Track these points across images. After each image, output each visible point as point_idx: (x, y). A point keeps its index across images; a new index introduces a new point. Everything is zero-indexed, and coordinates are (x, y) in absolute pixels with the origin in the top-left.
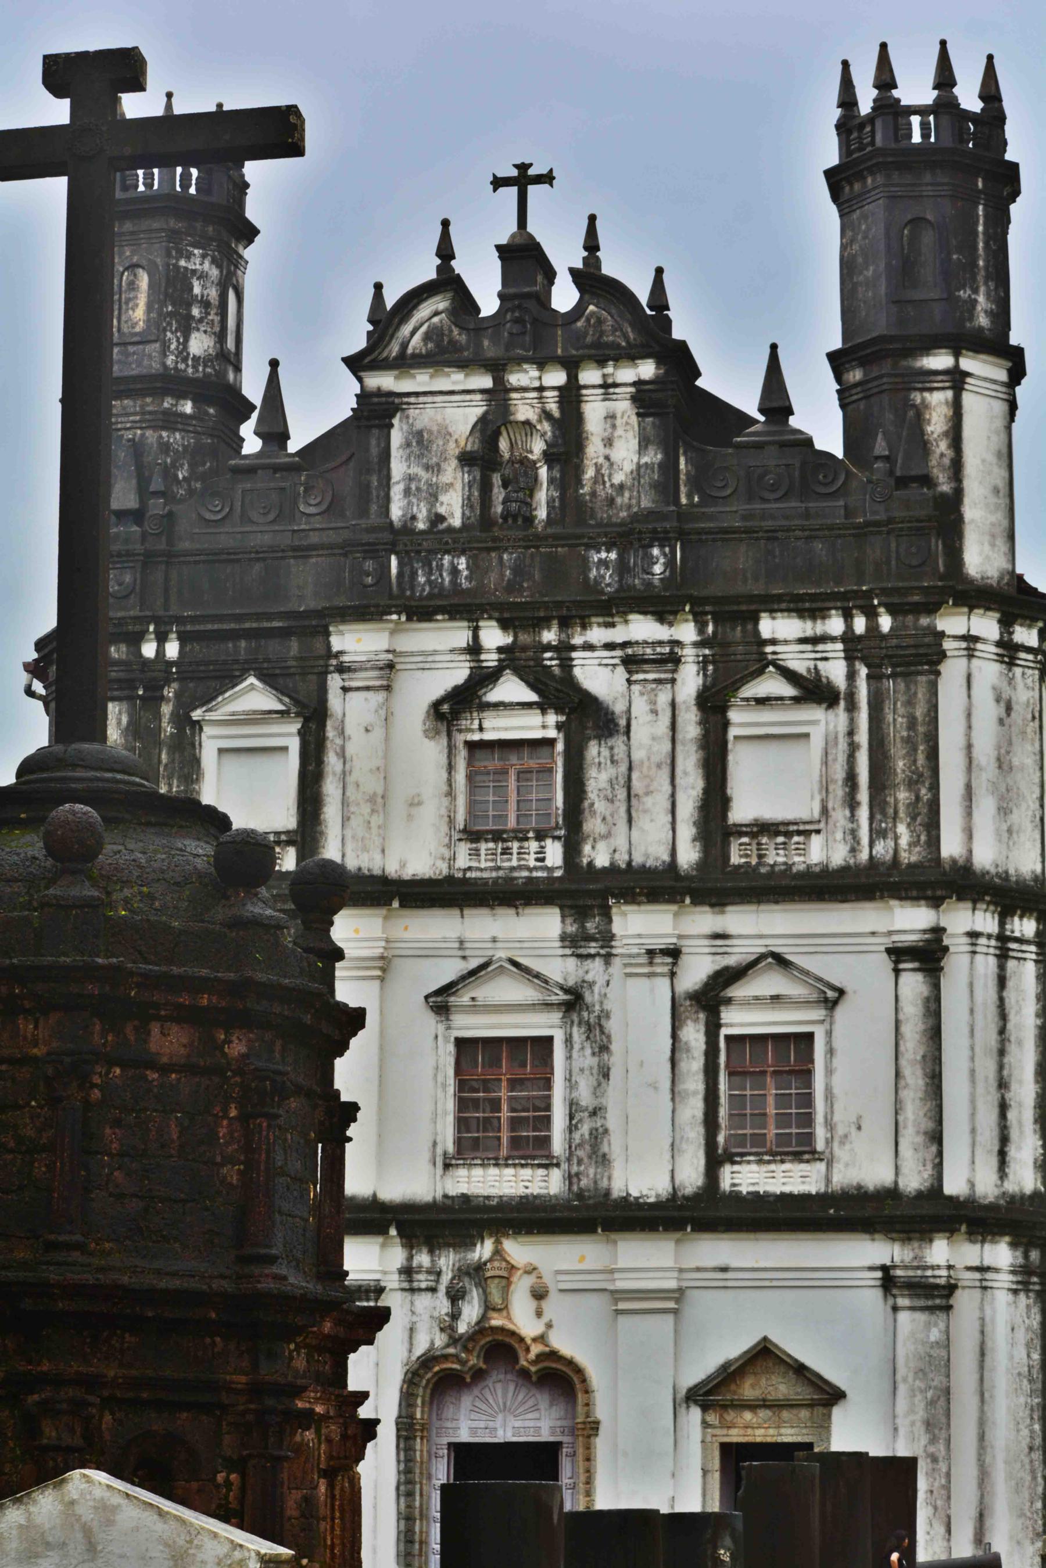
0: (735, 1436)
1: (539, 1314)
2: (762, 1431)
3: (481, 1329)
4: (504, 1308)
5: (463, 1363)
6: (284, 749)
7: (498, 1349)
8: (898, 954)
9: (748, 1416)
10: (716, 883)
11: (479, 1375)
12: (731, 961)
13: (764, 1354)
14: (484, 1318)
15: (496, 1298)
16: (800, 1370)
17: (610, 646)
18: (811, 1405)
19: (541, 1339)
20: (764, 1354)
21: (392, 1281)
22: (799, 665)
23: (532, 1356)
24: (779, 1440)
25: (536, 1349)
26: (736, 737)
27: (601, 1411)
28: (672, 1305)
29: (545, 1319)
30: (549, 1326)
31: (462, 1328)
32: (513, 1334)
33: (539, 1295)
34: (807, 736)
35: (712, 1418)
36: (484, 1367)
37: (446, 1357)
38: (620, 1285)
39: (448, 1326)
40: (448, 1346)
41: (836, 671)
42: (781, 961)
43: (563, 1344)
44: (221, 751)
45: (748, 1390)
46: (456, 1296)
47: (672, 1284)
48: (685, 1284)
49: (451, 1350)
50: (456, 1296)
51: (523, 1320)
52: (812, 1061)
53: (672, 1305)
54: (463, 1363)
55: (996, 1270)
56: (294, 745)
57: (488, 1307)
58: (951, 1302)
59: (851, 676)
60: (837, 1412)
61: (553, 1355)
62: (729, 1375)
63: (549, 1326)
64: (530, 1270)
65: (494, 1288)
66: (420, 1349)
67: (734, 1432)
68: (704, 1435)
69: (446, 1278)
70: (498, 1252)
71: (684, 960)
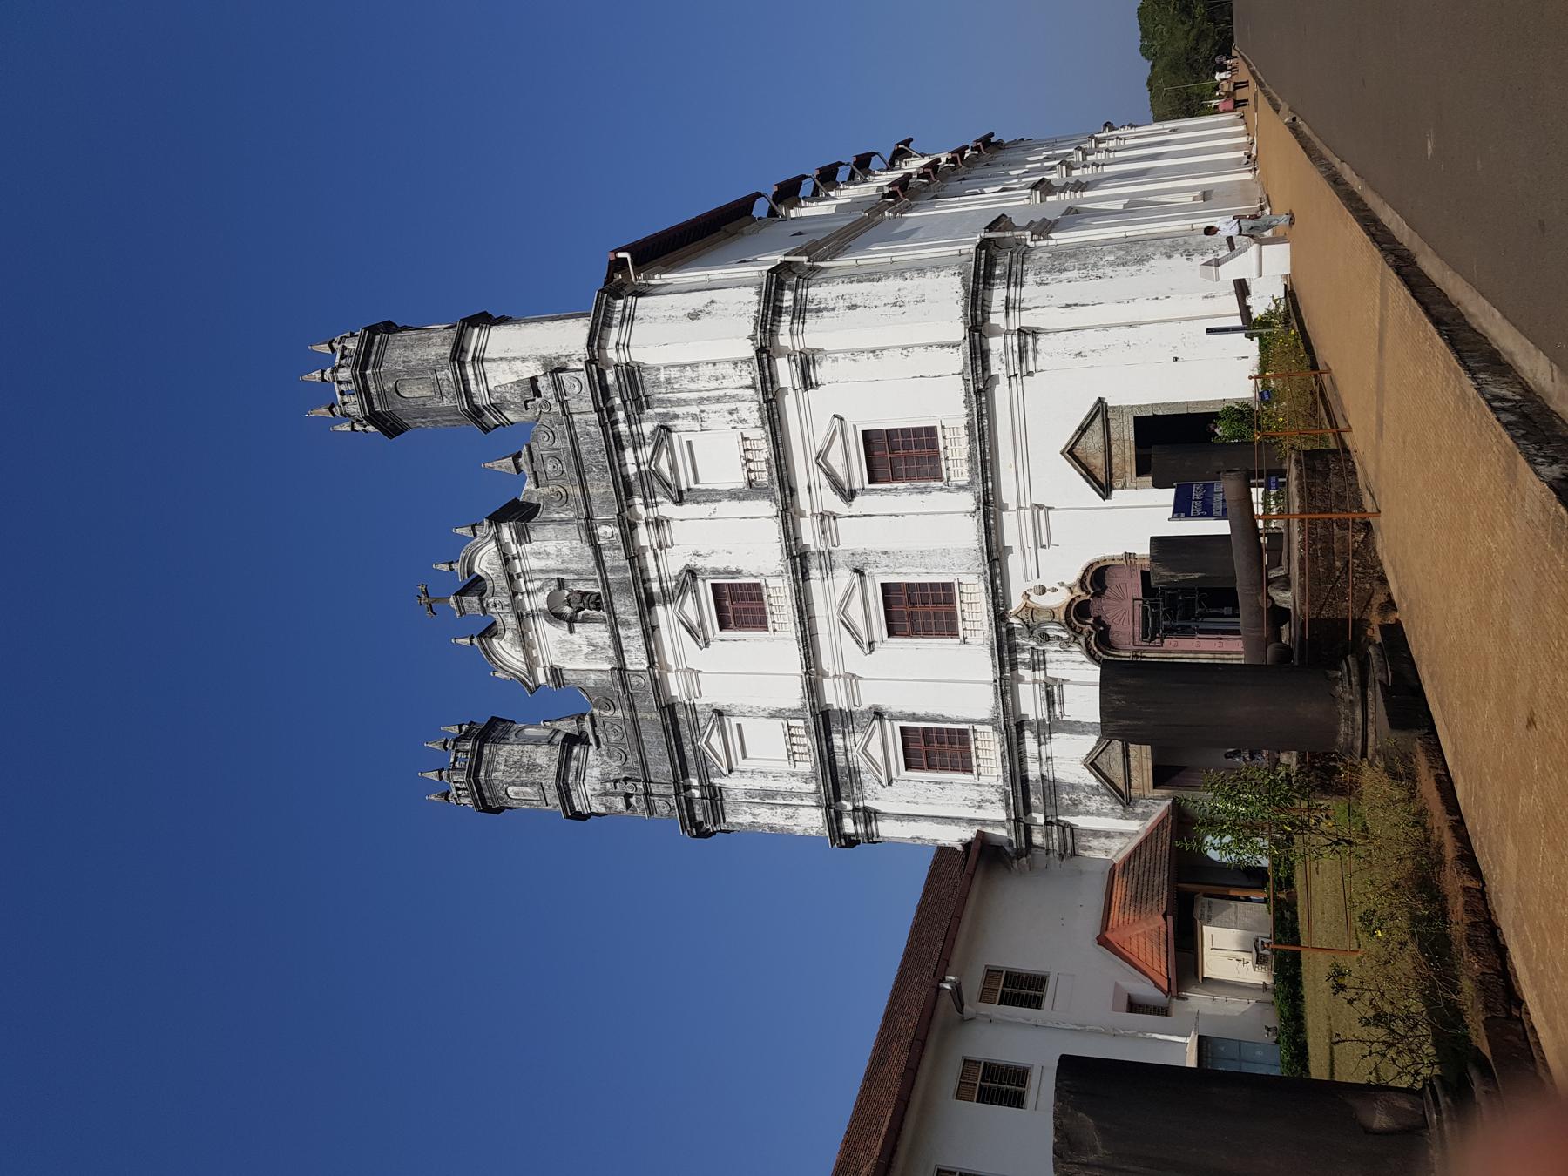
0: (1131, 468)
1: (1055, 590)
5: (1090, 633)
6: (739, 726)
7: (1078, 612)
8: (808, 383)
9: (1115, 460)
10: (783, 487)
11: (1098, 620)
12: (824, 481)
13: (1071, 453)
16: (1083, 430)
17: (656, 556)
20: (1071, 453)
21: (1040, 675)
22: (649, 450)
26: (696, 482)
30: (1062, 584)
32: (1069, 605)
33: (1043, 590)
34: (689, 443)
35: (1117, 483)
36: (1091, 621)
37: (1087, 643)
38: (1031, 544)
39: (1066, 645)
41: (647, 428)
42: (822, 456)
43: (1074, 576)
44: (744, 757)
45: (1097, 462)
46: (1046, 638)
47: (1029, 513)
49: (1082, 640)
50: (1046, 638)
51: (1059, 600)
54: (1090, 633)
55: (1007, 298)
56: (734, 721)
59: (650, 419)
61: (1082, 582)
62: (1089, 474)
63: (1062, 584)
65: (1040, 618)
66: (1084, 658)
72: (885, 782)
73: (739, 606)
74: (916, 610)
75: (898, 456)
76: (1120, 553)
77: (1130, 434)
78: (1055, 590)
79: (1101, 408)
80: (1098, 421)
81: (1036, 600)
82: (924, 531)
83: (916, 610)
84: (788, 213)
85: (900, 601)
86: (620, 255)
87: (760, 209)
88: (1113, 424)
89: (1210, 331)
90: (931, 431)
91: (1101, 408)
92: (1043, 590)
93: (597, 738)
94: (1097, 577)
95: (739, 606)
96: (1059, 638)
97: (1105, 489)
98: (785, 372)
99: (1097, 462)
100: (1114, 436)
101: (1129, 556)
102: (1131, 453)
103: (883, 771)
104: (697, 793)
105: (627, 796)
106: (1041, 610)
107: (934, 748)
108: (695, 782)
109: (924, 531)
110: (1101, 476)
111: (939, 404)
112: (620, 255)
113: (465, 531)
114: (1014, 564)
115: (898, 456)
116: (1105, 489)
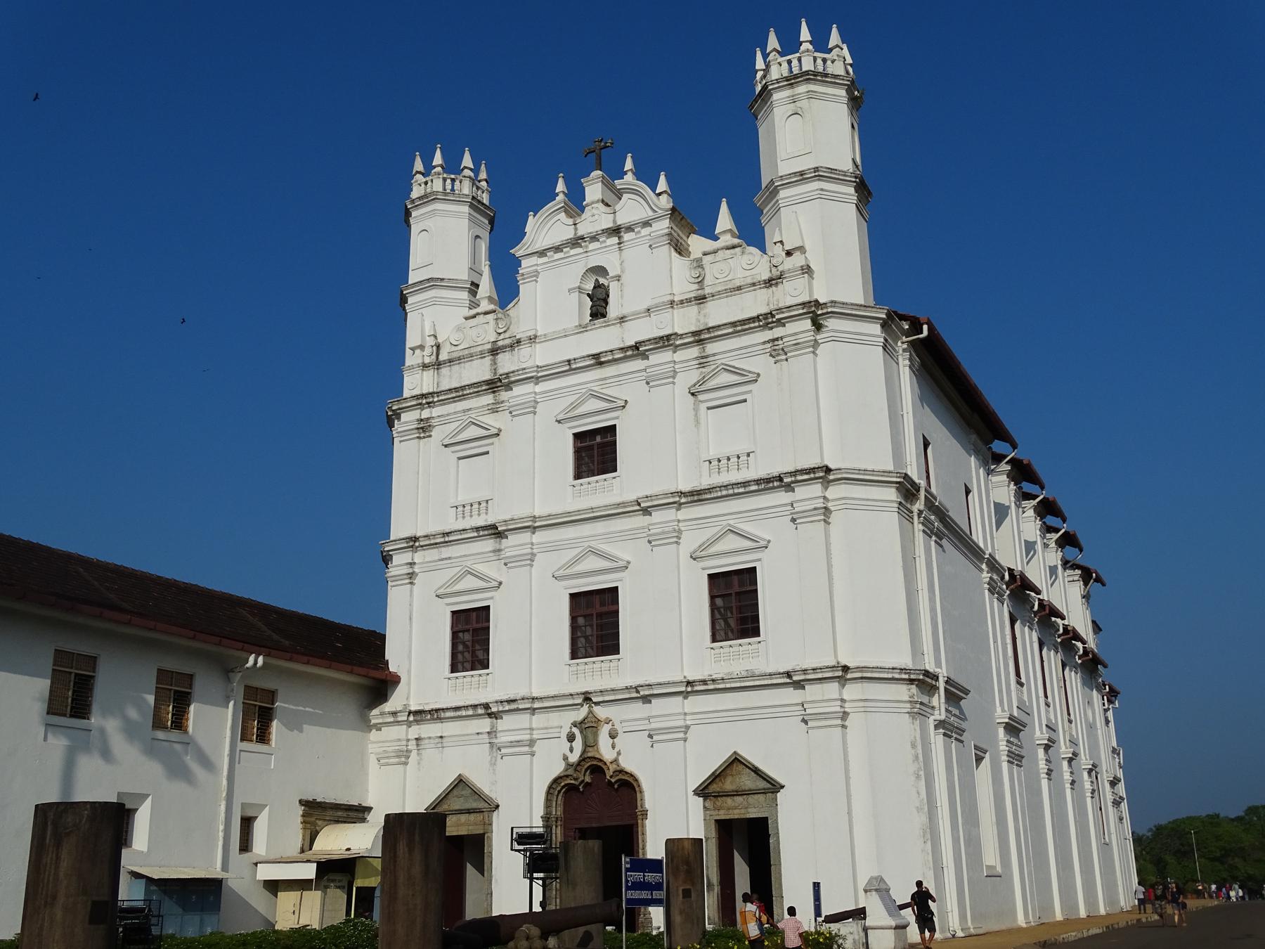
0: (723, 815)
1: (613, 747)
2: (736, 811)
3: (583, 759)
4: (595, 745)
5: (576, 779)
7: (596, 767)
9: (729, 800)
13: (736, 761)
14: (584, 752)
15: (591, 742)
16: (756, 771)
18: (764, 792)
19: (615, 761)
20: (736, 761)
23: (612, 770)
24: (748, 816)
25: (613, 768)
27: (648, 804)
28: (682, 735)
29: (617, 750)
30: (619, 753)
31: (574, 758)
32: (601, 760)
33: (613, 735)
37: (567, 776)
38: (653, 726)
40: (566, 770)
43: (627, 764)
45: (729, 785)
46: (571, 738)
47: (681, 723)
48: (688, 723)
49: (570, 772)
51: (606, 751)
52: (756, 584)
53: (682, 735)
57: (586, 746)
58: (846, 723)
60: (780, 795)
61: (621, 771)
62: (716, 777)
63: (619, 753)
64: (608, 721)
67: (722, 812)
68: (705, 815)
69: (566, 730)
70: (590, 712)
71: (683, 536)
72: (439, 592)
73: (596, 452)
74: (595, 622)
75: (735, 604)
76: (647, 806)
77: (753, 813)
78: (613, 747)
79: (774, 787)
80: (762, 784)
81: (604, 731)
82: (666, 625)
83: (595, 622)
84: (1001, 473)
85: (602, 604)
86: (925, 327)
87: (998, 446)
88: (761, 797)
89: (817, 886)
90: (756, 632)
91: (774, 787)
92: (613, 735)
93: (474, 317)
94: (627, 787)
95: (596, 452)
96: (571, 750)
97: (703, 791)
98: (809, 493)
99: (729, 785)
100: (752, 799)
101: (645, 814)
102: (735, 815)
103: (449, 590)
104: (426, 414)
105: (422, 347)
106: (596, 735)
107: (471, 638)
108: (436, 411)
109: (666, 625)
110: (715, 788)
111: (783, 638)
112: (925, 327)
113: (662, 185)
114: (638, 710)
115: (735, 604)
116: (703, 791)
